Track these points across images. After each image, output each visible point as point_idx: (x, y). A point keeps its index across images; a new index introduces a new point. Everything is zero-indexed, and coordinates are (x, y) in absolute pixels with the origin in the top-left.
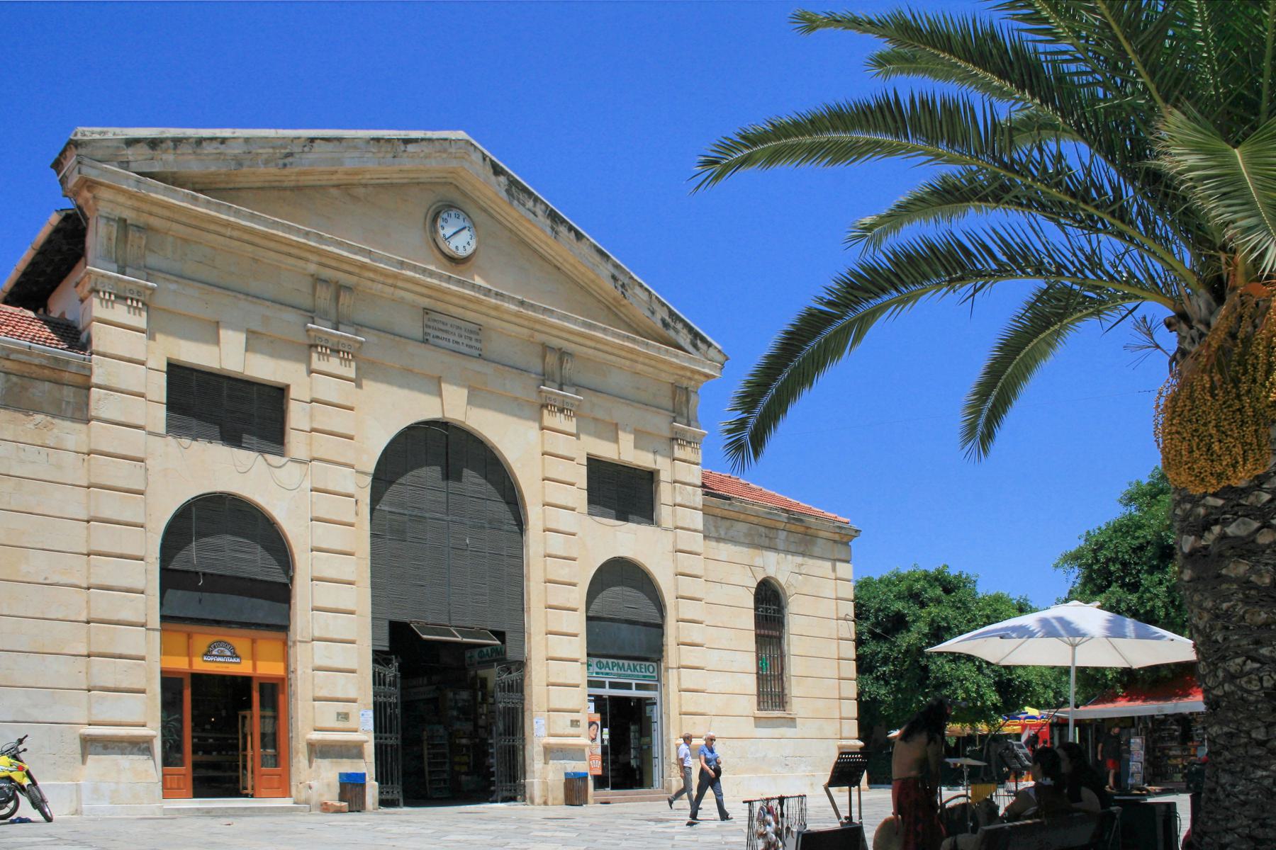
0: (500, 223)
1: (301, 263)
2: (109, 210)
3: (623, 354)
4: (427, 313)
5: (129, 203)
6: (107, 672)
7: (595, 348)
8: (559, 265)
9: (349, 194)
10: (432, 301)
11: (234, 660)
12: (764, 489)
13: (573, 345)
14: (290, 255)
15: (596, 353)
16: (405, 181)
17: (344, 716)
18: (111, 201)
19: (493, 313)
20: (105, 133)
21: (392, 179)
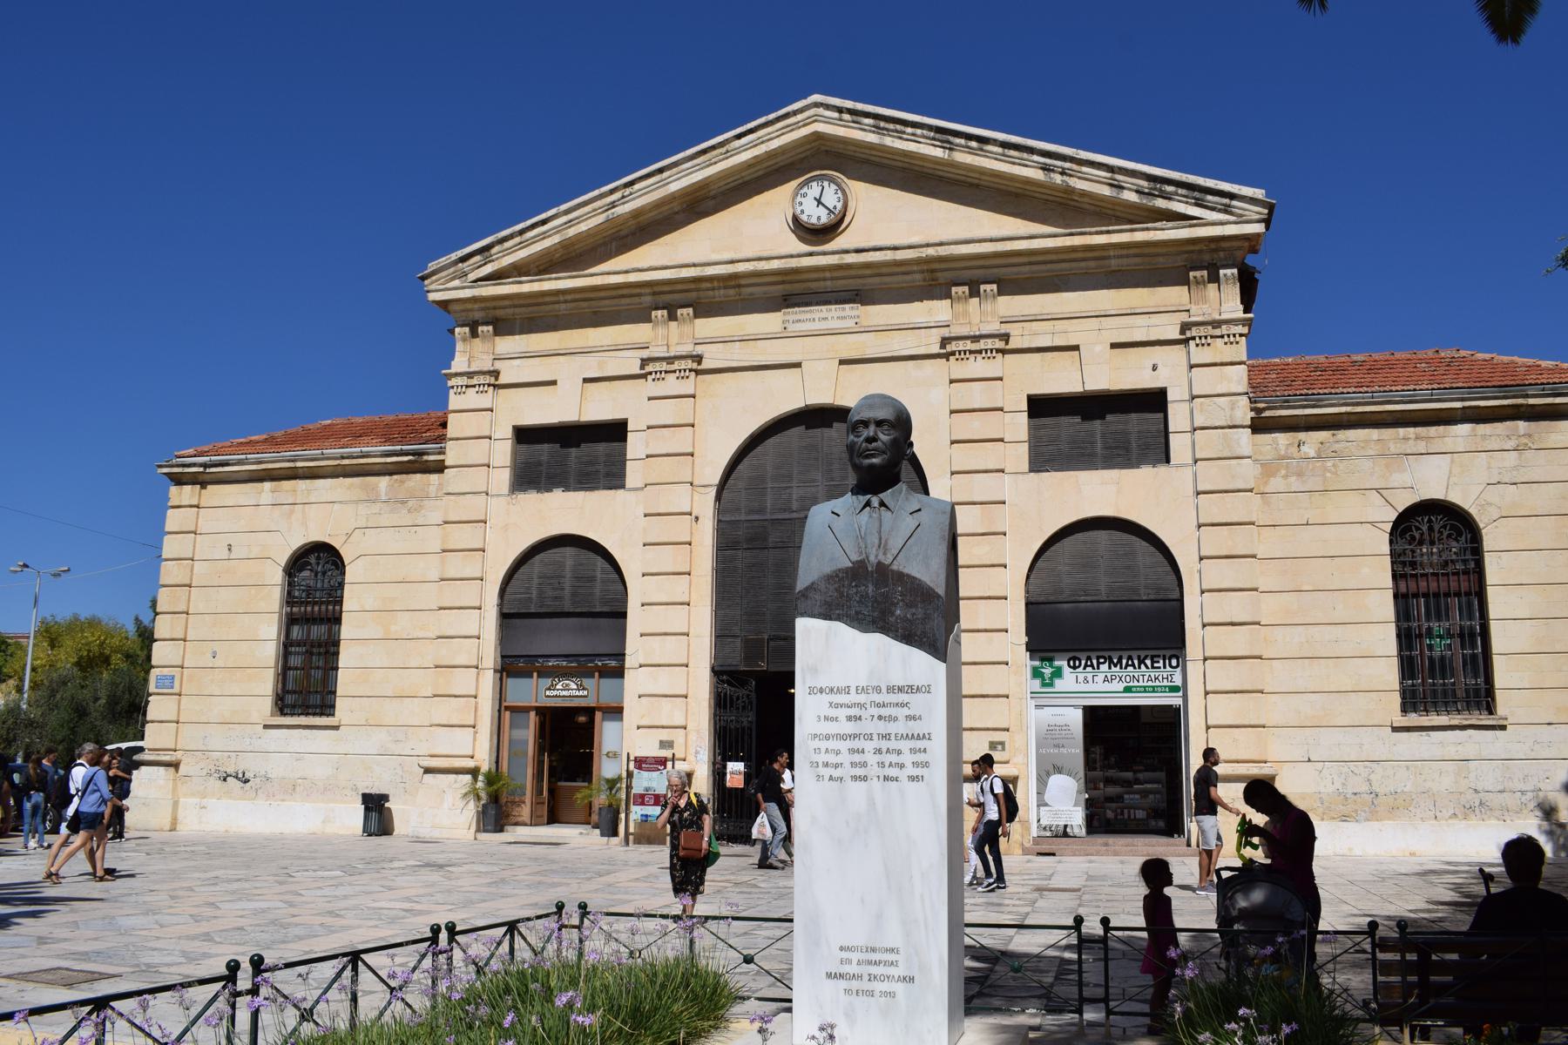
1: (636, 300)
2: (464, 318)
3: (1080, 255)
4: (785, 300)
5: (476, 306)
7: (1030, 263)
8: (976, 181)
10: (788, 287)
11: (581, 693)
12: (1497, 357)
13: (995, 270)
14: (623, 296)
15: (1035, 268)
16: (761, 173)
18: (463, 311)
19: (868, 272)
20: (450, 258)
21: (742, 177)
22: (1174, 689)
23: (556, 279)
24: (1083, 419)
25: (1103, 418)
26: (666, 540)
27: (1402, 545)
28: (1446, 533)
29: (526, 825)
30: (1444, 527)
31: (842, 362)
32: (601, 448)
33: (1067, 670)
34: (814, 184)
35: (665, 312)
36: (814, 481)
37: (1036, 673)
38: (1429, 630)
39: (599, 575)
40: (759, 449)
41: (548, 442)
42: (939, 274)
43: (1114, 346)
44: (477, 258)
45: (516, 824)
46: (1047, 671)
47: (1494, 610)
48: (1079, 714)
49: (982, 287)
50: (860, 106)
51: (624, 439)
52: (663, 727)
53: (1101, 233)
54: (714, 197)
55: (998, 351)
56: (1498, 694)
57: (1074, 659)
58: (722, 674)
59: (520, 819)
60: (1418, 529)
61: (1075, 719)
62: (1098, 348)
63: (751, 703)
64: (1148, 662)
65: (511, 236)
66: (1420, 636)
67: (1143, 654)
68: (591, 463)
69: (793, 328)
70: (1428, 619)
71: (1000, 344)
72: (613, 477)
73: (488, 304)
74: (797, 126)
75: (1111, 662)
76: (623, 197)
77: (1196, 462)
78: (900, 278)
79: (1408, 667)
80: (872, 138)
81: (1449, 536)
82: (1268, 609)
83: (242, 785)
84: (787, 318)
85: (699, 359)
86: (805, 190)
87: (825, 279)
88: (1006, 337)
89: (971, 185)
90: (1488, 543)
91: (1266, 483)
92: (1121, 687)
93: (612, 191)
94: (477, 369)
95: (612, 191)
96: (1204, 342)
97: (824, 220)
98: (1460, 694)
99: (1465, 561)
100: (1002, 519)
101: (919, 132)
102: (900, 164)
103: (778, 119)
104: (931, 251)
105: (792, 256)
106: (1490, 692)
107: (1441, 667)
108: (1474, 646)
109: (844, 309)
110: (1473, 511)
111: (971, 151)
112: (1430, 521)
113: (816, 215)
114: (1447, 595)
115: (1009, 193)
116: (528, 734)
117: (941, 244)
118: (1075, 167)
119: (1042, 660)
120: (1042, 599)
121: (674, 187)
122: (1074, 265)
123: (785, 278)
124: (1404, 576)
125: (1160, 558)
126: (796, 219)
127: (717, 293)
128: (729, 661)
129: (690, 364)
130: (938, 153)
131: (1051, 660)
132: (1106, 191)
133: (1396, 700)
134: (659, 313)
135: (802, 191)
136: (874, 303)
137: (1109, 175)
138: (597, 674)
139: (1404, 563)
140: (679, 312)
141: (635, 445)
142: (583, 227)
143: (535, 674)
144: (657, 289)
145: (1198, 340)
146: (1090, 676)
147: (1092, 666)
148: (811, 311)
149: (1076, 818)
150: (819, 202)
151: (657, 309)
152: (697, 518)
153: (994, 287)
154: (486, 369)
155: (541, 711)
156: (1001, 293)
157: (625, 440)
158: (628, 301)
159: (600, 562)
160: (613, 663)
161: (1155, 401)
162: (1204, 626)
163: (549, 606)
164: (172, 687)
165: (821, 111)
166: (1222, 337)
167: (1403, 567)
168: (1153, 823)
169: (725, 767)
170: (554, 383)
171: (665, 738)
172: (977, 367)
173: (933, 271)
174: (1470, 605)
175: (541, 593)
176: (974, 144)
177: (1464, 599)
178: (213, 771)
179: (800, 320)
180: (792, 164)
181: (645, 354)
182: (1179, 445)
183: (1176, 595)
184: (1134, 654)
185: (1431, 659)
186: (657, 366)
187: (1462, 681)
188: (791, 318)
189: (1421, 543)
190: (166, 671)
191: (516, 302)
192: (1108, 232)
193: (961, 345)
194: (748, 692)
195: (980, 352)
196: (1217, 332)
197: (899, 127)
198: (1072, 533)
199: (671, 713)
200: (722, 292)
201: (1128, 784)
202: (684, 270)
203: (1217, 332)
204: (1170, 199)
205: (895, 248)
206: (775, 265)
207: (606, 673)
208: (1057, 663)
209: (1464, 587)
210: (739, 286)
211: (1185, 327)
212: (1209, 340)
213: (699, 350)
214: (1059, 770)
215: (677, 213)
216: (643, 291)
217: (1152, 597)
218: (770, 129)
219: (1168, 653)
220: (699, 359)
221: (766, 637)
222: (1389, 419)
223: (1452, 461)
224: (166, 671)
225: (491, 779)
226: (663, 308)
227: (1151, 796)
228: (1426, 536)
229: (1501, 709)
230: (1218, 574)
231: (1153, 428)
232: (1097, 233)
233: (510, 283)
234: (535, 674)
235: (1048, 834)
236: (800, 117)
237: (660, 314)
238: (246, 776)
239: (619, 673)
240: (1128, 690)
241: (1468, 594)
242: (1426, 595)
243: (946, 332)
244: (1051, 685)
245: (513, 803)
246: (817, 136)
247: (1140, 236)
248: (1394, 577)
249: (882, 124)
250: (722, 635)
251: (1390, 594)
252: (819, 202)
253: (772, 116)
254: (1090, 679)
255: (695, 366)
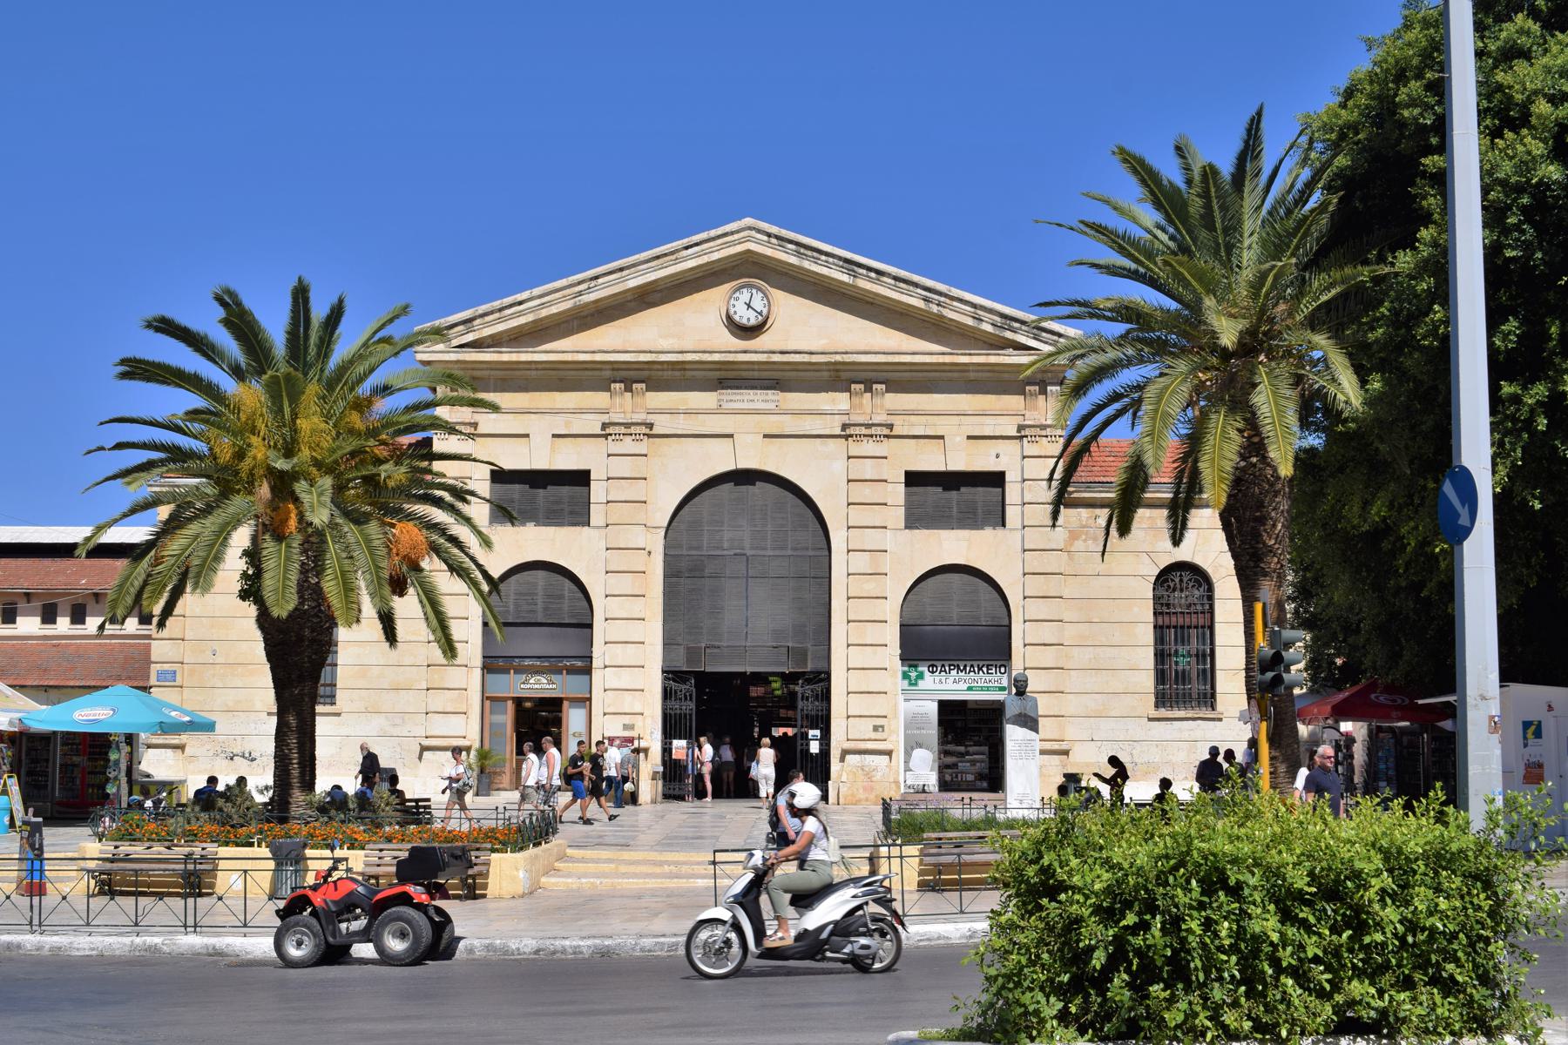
0: (803, 280)
6: (438, 701)
7: (911, 371)
9: (645, 302)
14: (586, 369)
16: (701, 274)
17: (626, 727)
22: (1002, 689)
23: (532, 352)
24: (944, 489)
25: (959, 490)
26: (626, 569)
27: (1162, 592)
28: (1191, 584)
29: (506, 790)
30: (1190, 580)
31: (765, 436)
32: (565, 491)
33: (927, 674)
34: (745, 290)
35: (622, 385)
36: (741, 526)
37: (905, 676)
38: (1176, 651)
39: (567, 595)
40: (697, 500)
41: (519, 483)
42: (842, 374)
43: (969, 437)
44: (461, 328)
45: (498, 789)
46: (913, 675)
47: (1218, 640)
48: (935, 706)
49: (875, 386)
50: (785, 233)
51: (588, 485)
52: (625, 714)
53: (965, 354)
54: (661, 291)
55: (885, 436)
56: (1218, 697)
57: (933, 666)
58: (672, 676)
59: (501, 786)
60: (1173, 580)
61: (932, 709)
62: (958, 439)
63: (691, 695)
64: (985, 669)
65: (492, 312)
66: (1170, 655)
67: (981, 663)
68: (557, 503)
69: (725, 405)
70: (1176, 644)
71: (886, 431)
72: (579, 515)
73: (469, 366)
74: (733, 243)
75: (959, 668)
76: (589, 288)
77: (1024, 527)
78: (812, 374)
79: (1161, 677)
80: (793, 260)
81: (1193, 586)
82: (1069, 633)
83: (249, 763)
84: (721, 397)
85: (651, 426)
86: (737, 294)
87: (753, 370)
88: (891, 427)
89: (868, 302)
90: (1218, 593)
91: (1071, 545)
92: (965, 687)
93: (580, 283)
94: (459, 420)
95: (580, 283)
96: (1034, 440)
97: (753, 322)
98: (1195, 696)
99: (1202, 604)
100: (886, 564)
101: (831, 260)
102: (813, 280)
103: (719, 237)
104: (838, 358)
105: (730, 352)
106: (1213, 696)
107: (1183, 677)
108: (1205, 664)
109: (767, 394)
110: (1210, 571)
111: (870, 280)
112: (1181, 575)
113: (746, 317)
114: (1189, 627)
115: (896, 312)
116: (507, 718)
117: (846, 353)
118: (948, 301)
119: (910, 666)
120: (911, 622)
121: (632, 284)
122: (943, 374)
123: (723, 367)
124: (1161, 613)
125: (996, 595)
126: (729, 317)
127: (665, 373)
128: (675, 664)
129: (644, 430)
130: (845, 278)
131: (916, 666)
132: (970, 322)
133: (1152, 699)
134: (618, 385)
135: (735, 296)
136: (790, 391)
137: (973, 310)
138: (565, 672)
139: (1162, 604)
140: (634, 386)
141: (597, 491)
142: (554, 310)
143: (512, 671)
144: (616, 366)
145: (1029, 438)
146: (943, 679)
147: (945, 671)
148: (741, 394)
149: (931, 779)
150: (749, 306)
151: (615, 382)
152: (650, 553)
153: (884, 386)
154: (467, 421)
155: (518, 701)
156: (887, 391)
157: (589, 485)
158: (590, 373)
159: (567, 583)
160: (579, 664)
161: (996, 479)
162: (1025, 645)
163: (524, 617)
164: (175, 681)
165: (753, 233)
166: (1047, 436)
167: (1161, 607)
168: (978, 783)
169: (671, 743)
170: (527, 436)
171: (627, 722)
172: (869, 447)
173: (837, 371)
174: (1204, 634)
175: (517, 606)
176: (873, 275)
177: (1200, 630)
178: (220, 751)
179: (731, 401)
180: (725, 270)
181: (605, 418)
182: (1012, 513)
183: (1006, 622)
184: (975, 663)
185: (1176, 671)
186: (617, 430)
187: (1195, 687)
188: (725, 398)
189: (1174, 590)
190: (166, 667)
191: (493, 366)
192: (970, 354)
193: (857, 430)
194: (689, 687)
195: (871, 436)
196: (1044, 433)
197: (815, 254)
198: (934, 575)
199: (629, 703)
200: (670, 373)
201: (962, 755)
202: (642, 355)
203: (1044, 433)
204: (1015, 332)
205: (811, 353)
206: (716, 357)
207: (572, 671)
208: (920, 669)
209: (1201, 622)
210: (685, 369)
211: (1020, 428)
212: (1038, 439)
213: (651, 418)
214: (920, 746)
215: (630, 301)
216: (604, 367)
217: (989, 623)
218: (712, 244)
219: (999, 663)
220: (651, 426)
221: (703, 645)
222: (1158, 503)
223: (1198, 535)
224: (166, 667)
225: (483, 755)
226: (621, 382)
227: (978, 764)
228: (1178, 586)
229: (1220, 706)
230: (1037, 609)
231: (995, 499)
232: (962, 354)
233: (494, 352)
234: (512, 671)
235: (912, 791)
236: (736, 236)
237: (617, 386)
238: (253, 756)
239: (587, 671)
240: (970, 689)
241: (1203, 627)
242: (1175, 627)
243: (845, 419)
244: (916, 684)
245: (495, 773)
246: (749, 251)
247: (993, 359)
248: (1155, 613)
249: (802, 250)
250: (668, 643)
251: (1151, 627)
252: (749, 306)
253: (713, 233)
254: (944, 681)
255: (648, 431)
